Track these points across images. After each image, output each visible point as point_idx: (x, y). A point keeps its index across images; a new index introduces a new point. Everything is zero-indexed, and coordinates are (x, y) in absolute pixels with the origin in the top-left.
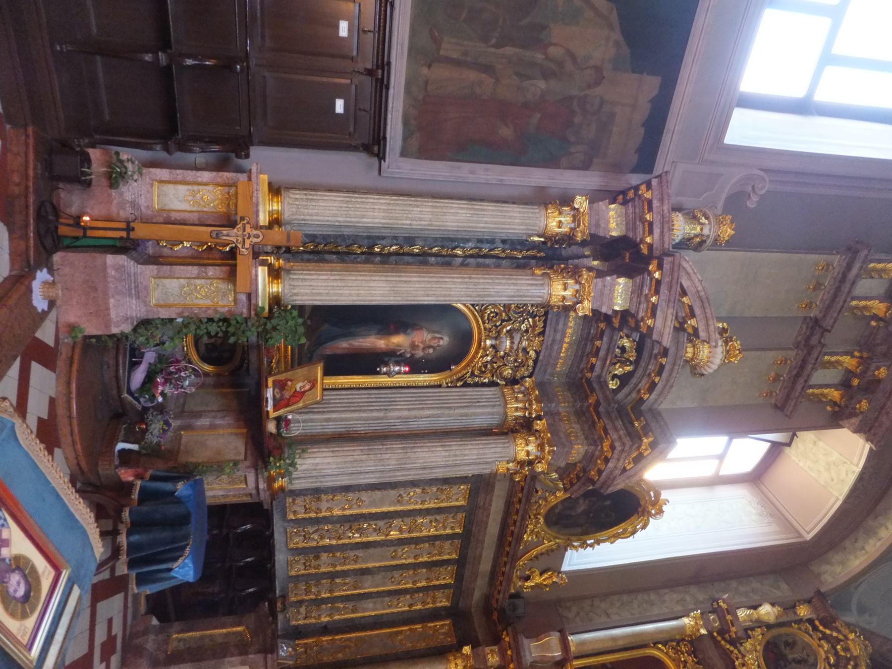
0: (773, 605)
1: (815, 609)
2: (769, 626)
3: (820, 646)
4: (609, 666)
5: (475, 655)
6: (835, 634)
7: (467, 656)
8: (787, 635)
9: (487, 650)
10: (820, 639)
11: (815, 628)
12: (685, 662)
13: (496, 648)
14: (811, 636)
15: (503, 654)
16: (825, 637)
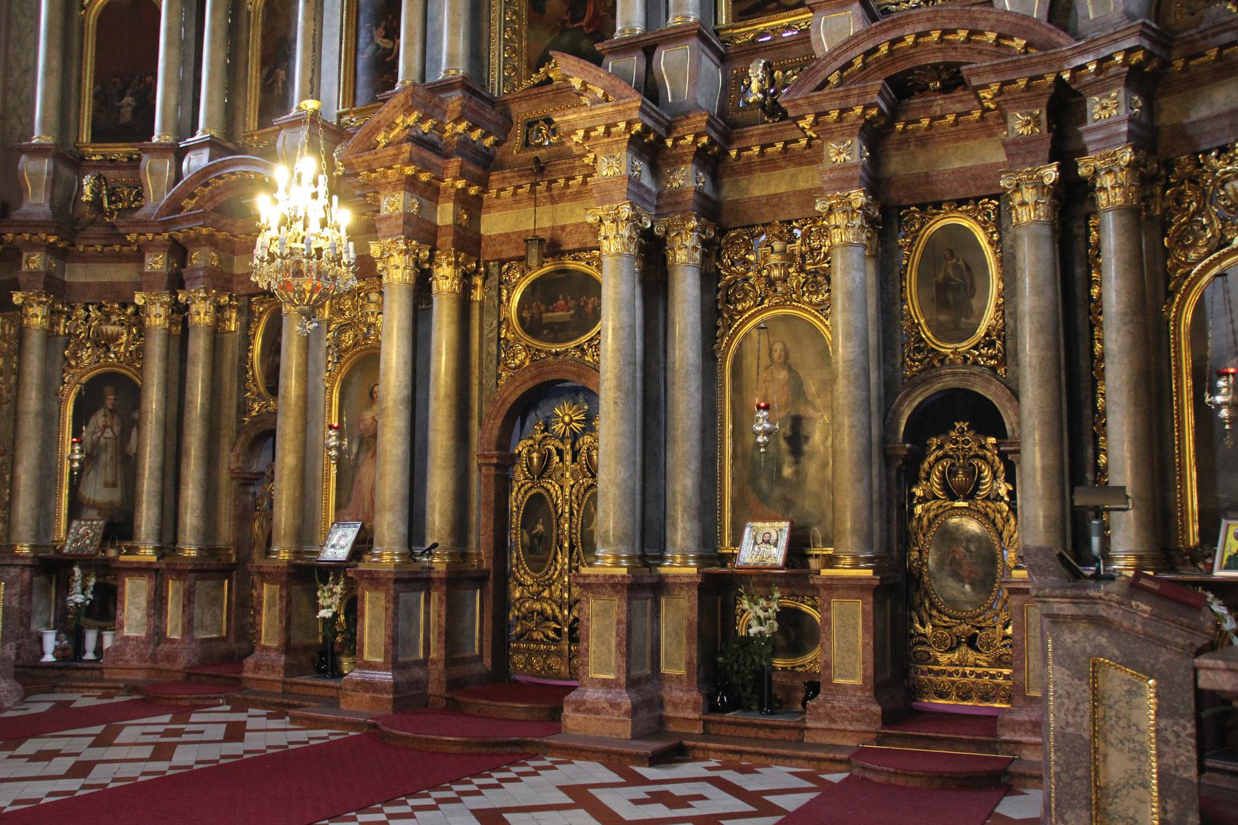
4: (99, 87)
9: (25, 268)
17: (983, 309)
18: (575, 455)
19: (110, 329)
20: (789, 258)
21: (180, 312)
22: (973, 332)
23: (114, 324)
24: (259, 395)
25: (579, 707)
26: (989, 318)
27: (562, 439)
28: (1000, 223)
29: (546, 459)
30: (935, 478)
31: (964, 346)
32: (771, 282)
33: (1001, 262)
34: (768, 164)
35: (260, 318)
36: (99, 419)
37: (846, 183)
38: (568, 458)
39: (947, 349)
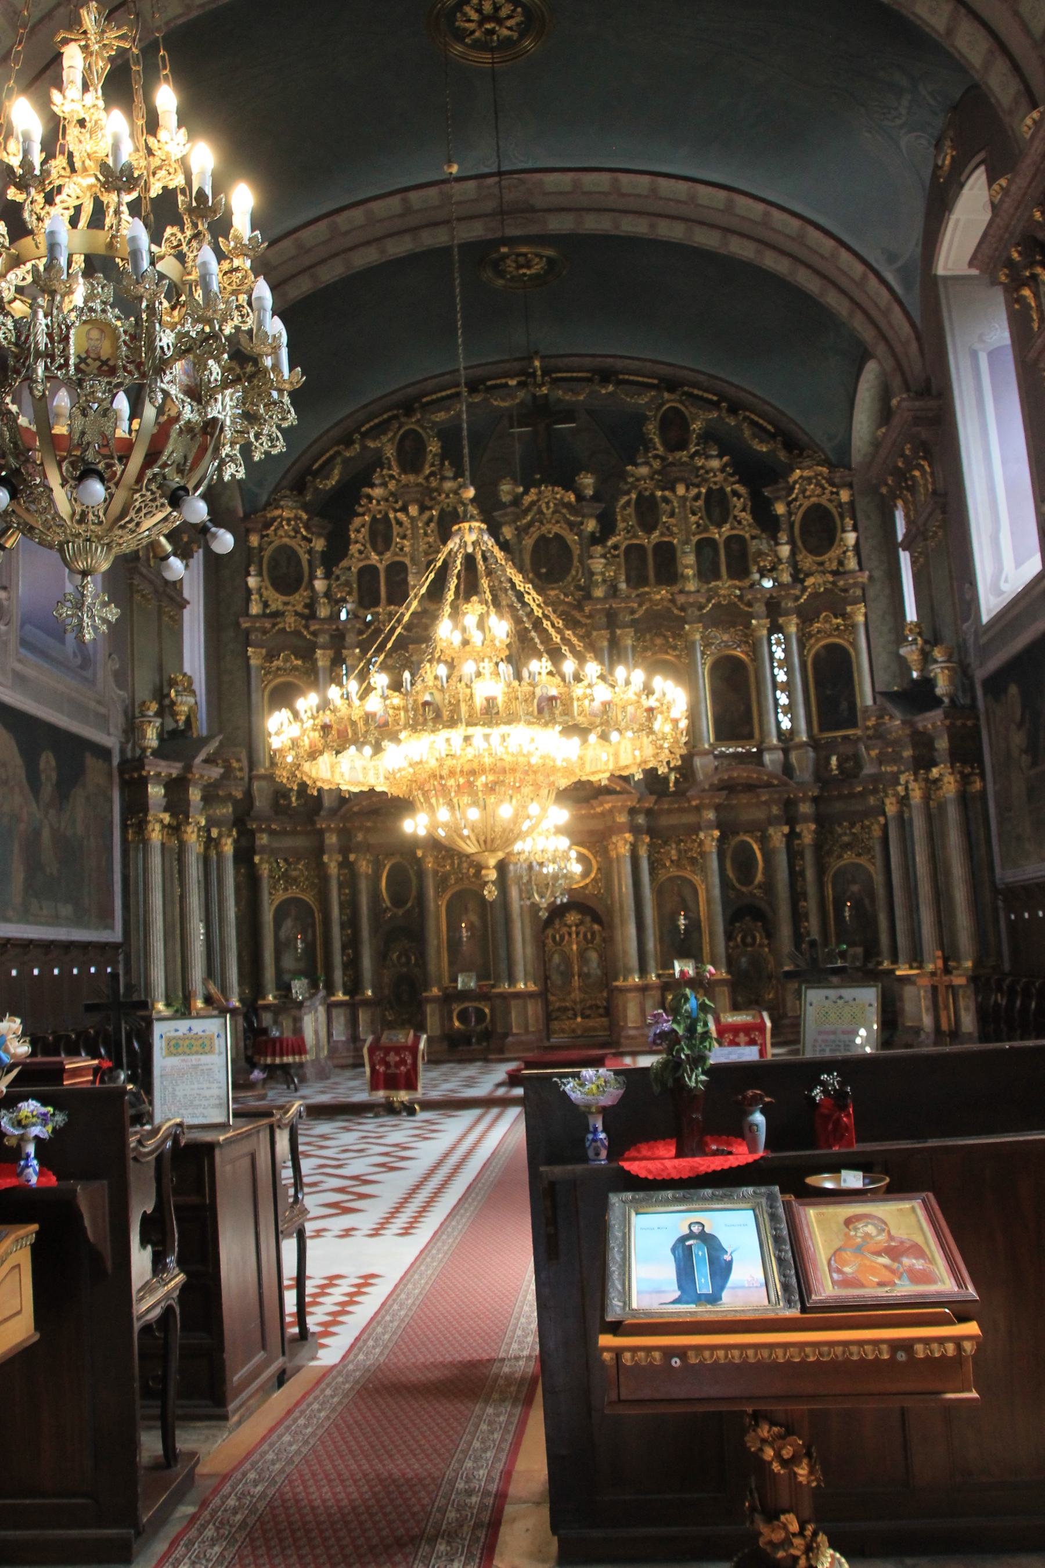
0: (248, 574)
1: (254, 530)
2: (263, 581)
3: (281, 537)
5: (261, 853)
6: (276, 524)
7: (261, 859)
8: (269, 563)
9: (258, 842)
10: (276, 535)
11: (267, 535)
12: (278, 669)
13: (258, 835)
14: (271, 543)
15: (262, 831)
16: (275, 530)
17: (755, 876)
18: (578, 934)
19: (294, 873)
20: (679, 851)
21: (345, 864)
22: (751, 882)
23: (295, 869)
24: (387, 908)
25: (629, 1037)
26: (759, 877)
27: (570, 927)
28: (764, 840)
29: (562, 938)
30: (739, 939)
31: (750, 888)
32: (672, 861)
33: (764, 855)
34: (670, 811)
35: (385, 866)
36: (288, 924)
37: (710, 827)
38: (574, 936)
39: (744, 889)
